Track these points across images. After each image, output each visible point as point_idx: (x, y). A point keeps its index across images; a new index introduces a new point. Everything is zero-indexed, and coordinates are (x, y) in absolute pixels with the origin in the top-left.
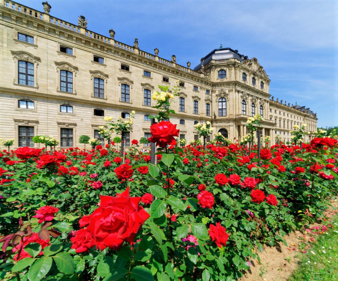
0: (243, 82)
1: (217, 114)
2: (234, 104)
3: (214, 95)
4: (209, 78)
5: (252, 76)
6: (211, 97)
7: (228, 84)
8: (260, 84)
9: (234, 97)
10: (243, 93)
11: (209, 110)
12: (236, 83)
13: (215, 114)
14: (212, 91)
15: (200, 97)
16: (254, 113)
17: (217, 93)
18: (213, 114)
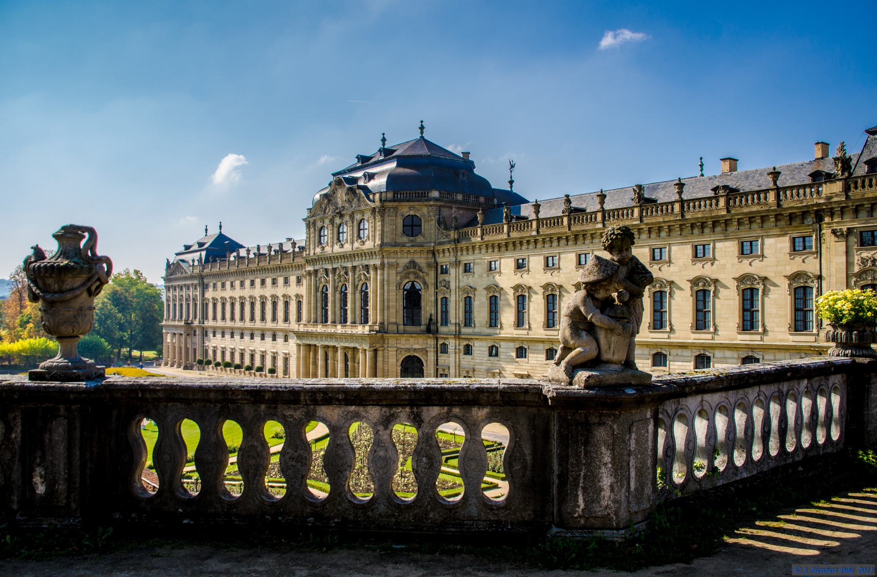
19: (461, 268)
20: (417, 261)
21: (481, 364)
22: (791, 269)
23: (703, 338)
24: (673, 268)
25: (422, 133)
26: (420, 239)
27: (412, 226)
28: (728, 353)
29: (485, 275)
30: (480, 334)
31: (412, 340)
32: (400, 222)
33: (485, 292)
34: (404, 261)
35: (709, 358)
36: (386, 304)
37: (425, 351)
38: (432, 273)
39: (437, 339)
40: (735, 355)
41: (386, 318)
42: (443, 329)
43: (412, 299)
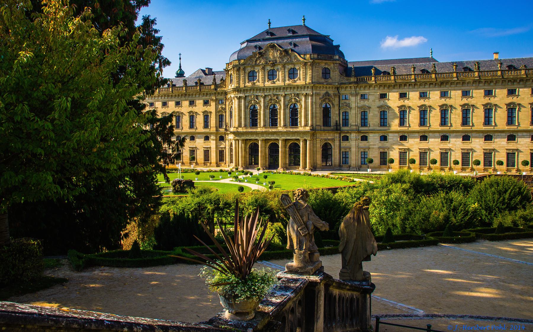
0: (249, 85)
3: (227, 103)
19: (359, 97)
20: (329, 92)
21: (374, 145)
22: (462, 103)
24: (496, 99)
26: (330, 81)
27: (326, 73)
28: (525, 134)
30: (374, 130)
31: (327, 134)
32: (321, 72)
33: (378, 109)
34: (323, 92)
35: (492, 136)
36: (314, 115)
37: (333, 140)
39: (340, 134)
40: (528, 134)
41: (314, 123)
43: (326, 112)
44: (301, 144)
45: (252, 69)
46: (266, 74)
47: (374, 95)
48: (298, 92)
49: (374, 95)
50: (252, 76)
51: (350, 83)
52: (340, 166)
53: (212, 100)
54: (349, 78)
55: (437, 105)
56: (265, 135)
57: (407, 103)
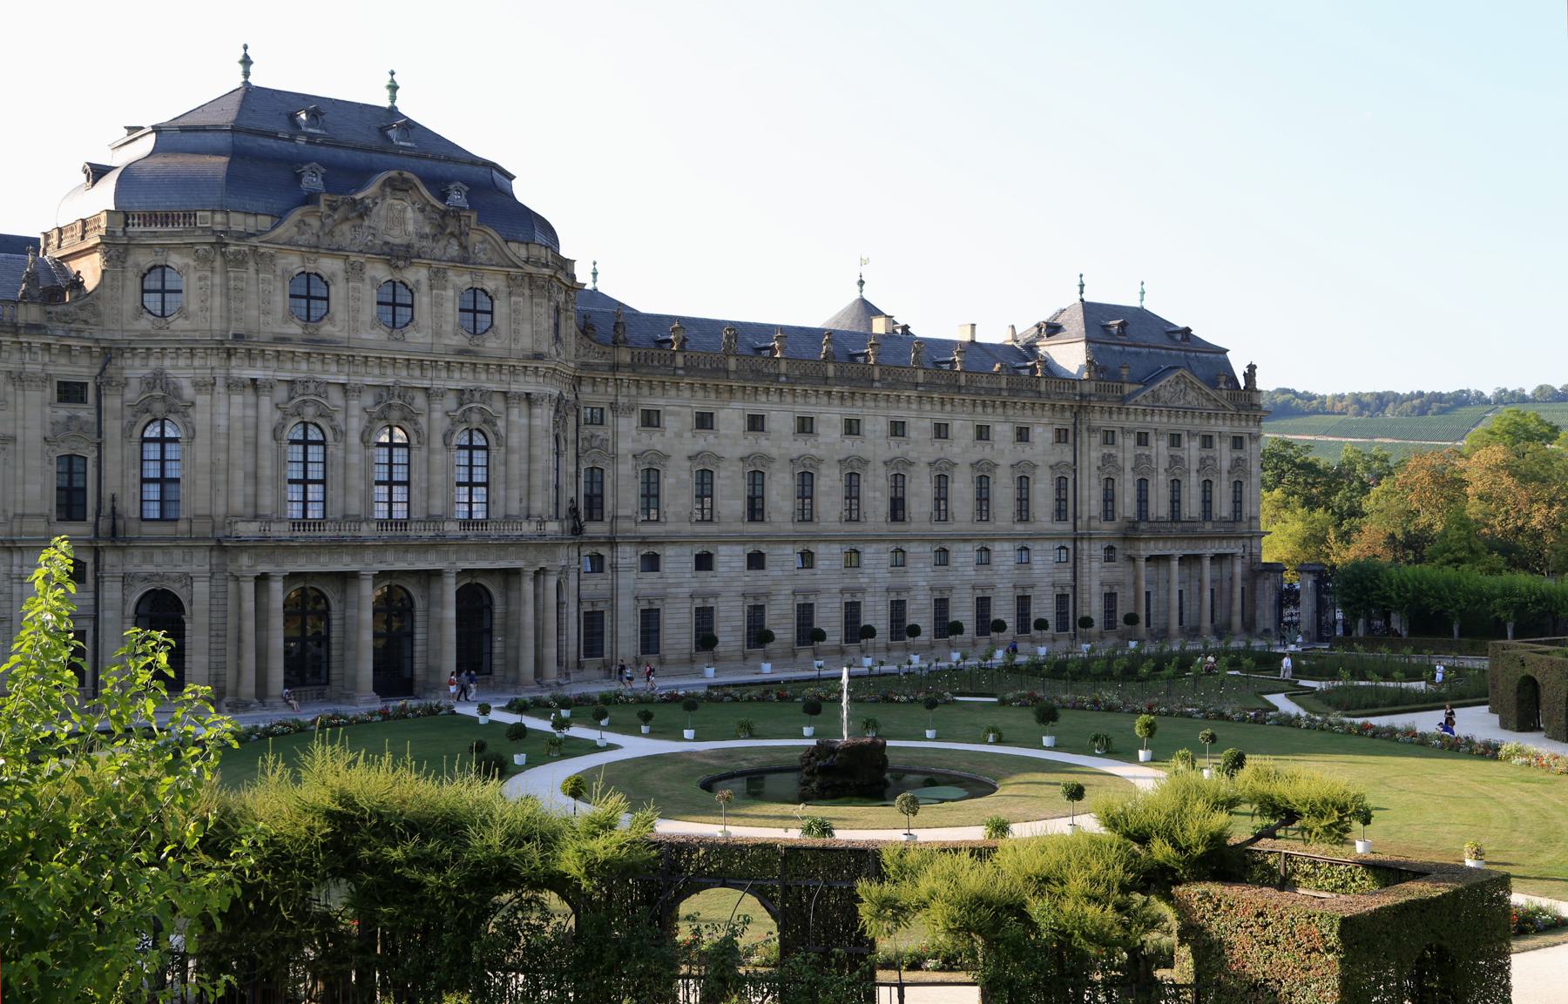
0: (295, 329)
1: (129, 507)
2: (222, 456)
3: (112, 402)
4: (83, 315)
5: (381, 272)
6: (93, 418)
7: (191, 348)
8: (450, 309)
9: (222, 422)
10: (299, 389)
11: (84, 490)
12: (233, 346)
13: (113, 508)
14: (98, 389)
15: (10, 432)
16: (407, 483)
17: (132, 394)
18: (107, 509)
19: (636, 419)
21: (679, 585)
23: (986, 528)
24: (956, 450)
25: (393, 98)
29: (688, 435)
38: (571, 421)
42: (592, 529)
44: (528, 586)
45: (310, 268)
46: (369, 295)
47: (677, 414)
48: (493, 387)
49: (677, 414)
50: (309, 294)
51: (615, 367)
52: (580, 666)
53: (18, 379)
54: (608, 350)
55: (836, 458)
56: (390, 556)
57: (764, 444)
